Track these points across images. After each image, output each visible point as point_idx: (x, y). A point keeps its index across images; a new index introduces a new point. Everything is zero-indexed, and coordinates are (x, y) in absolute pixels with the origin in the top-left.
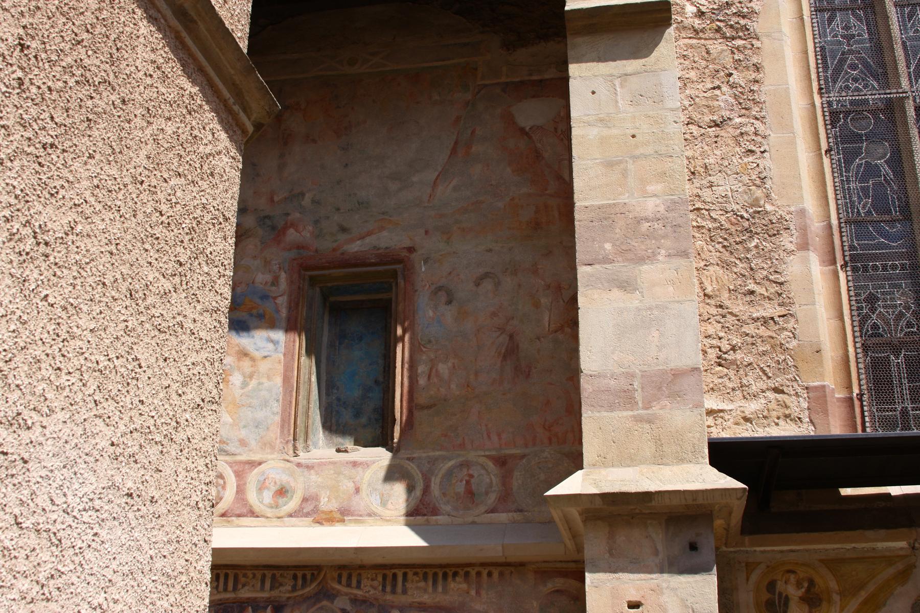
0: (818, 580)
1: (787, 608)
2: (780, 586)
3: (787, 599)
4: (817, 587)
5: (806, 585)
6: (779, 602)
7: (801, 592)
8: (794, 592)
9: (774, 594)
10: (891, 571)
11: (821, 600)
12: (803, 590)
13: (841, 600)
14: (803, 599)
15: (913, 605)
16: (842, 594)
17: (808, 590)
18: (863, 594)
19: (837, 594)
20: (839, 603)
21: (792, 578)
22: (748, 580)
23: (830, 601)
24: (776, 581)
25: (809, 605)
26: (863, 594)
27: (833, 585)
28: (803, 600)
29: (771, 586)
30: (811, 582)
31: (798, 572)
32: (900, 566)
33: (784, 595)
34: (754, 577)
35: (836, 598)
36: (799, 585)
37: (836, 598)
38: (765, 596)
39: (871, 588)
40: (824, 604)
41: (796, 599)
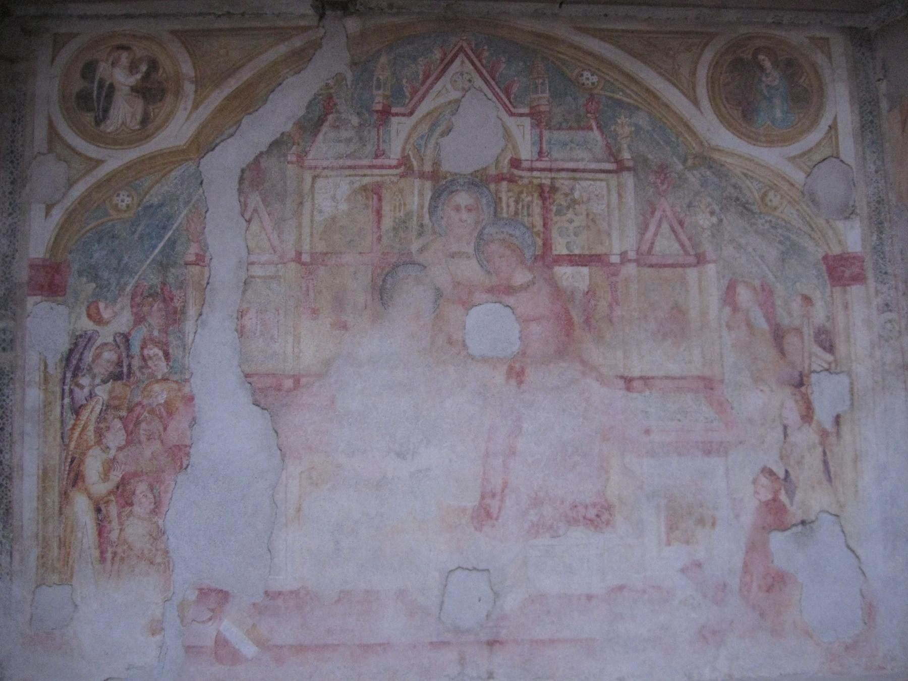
0: (163, 59)
1: (111, 103)
2: (103, 69)
3: (112, 87)
4: (161, 71)
5: (144, 68)
6: (99, 94)
7: (133, 80)
8: (123, 79)
9: (92, 82)
10: (283, 49)
11: (163, 91)
12: (139, 76)
13: (196, 91)
14: (134, 89)
15: (310, 102)
16: (199, 82)
17: (147, 75)
18: (232, 85)
19: (192, 82)
20: (192, 97)
21: (125, 58)
22: (53, 59)
23: (178, 93)
24: (97, 61)
25: (144, 98)
26: (232, 85)
27: (187, 69)
28: (137, 92)
29: (89, 70)
30: (153, 65)
31: (135, 48)
32: (297, 42)
33: (107, 83)
34: (65, 55)
35: (189, 88)
36: (133, 68)
37: (189, 88)
38: (78, 85)
39: (246, 75)
40: (169, 98)
41: (126, 89)
